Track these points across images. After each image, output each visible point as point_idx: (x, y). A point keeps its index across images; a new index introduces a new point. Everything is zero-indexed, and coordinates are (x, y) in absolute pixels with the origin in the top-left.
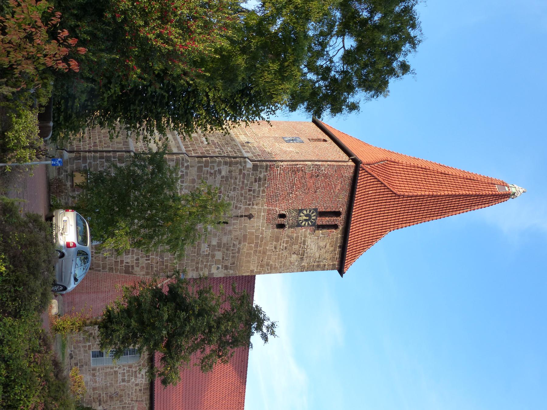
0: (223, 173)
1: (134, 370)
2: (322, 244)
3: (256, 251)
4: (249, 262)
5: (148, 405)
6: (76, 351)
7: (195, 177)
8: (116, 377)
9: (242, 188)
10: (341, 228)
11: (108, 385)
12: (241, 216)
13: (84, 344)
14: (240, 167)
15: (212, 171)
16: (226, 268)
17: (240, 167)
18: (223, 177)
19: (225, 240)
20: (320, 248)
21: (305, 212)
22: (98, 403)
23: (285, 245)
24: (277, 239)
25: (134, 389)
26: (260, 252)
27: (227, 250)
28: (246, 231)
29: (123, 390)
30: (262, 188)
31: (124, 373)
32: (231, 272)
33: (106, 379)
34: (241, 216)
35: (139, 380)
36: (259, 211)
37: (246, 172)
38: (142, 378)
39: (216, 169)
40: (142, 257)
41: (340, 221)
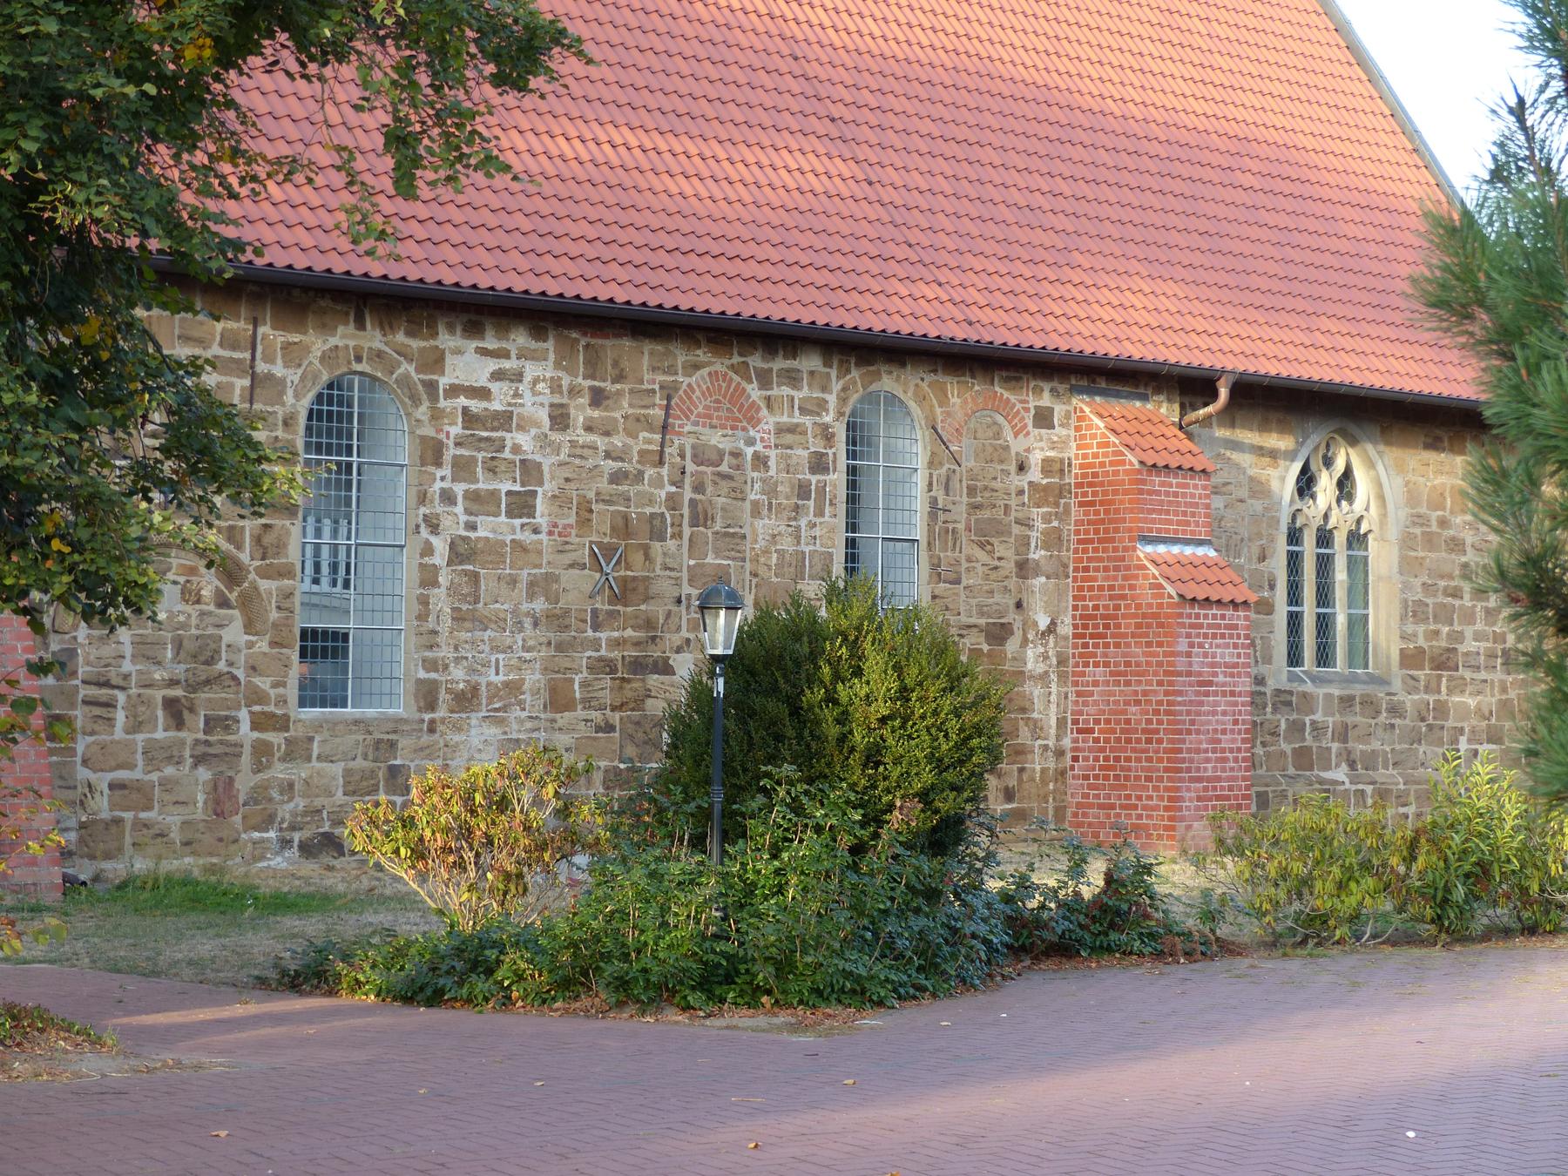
1: (456, 430)
5: (701, 354)
6: (285, 811)
8: (494, 551)
11: (539, 605)
13: (246, 759)
22: (654, 680)
25: (585, 438)
29: (585, 509)
31: (473, 497)
33: (500, 623)
35: (528, 399)
38: (518, 377)
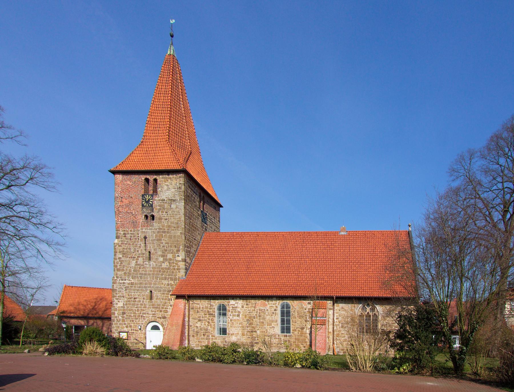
0: (121, 256)
2: (166, 187)
3: (168, 232)
4: (175, 237)
7: (123, 272)
9: (129, 244)
10: (155, 177)
12: (145, 243)
14: (117, 247)
15: (120, 263)
16: (178, 251)
17: (117, 247)
18: (123, 256)
19: (160, 253)
20: (168, 189)
21: (144, 203)
23: (165, 213)
24: (160, 219)
26: (168, 229)
27: (166, 251)
28: (154, 240)
30: (130, 232)
32: (181, 247)
34: (145, 243)
36: (143, 232)
37: (120, 243)
39: (118, 260)
40: (170, 303)
41: (151, 178)
